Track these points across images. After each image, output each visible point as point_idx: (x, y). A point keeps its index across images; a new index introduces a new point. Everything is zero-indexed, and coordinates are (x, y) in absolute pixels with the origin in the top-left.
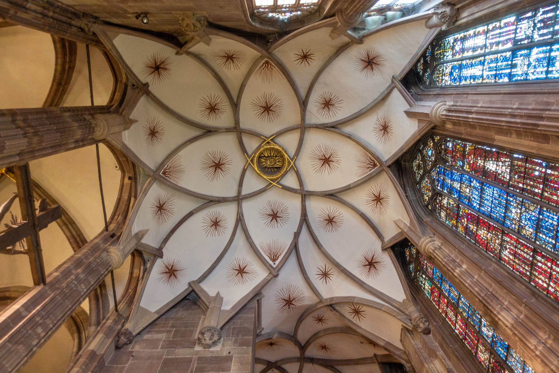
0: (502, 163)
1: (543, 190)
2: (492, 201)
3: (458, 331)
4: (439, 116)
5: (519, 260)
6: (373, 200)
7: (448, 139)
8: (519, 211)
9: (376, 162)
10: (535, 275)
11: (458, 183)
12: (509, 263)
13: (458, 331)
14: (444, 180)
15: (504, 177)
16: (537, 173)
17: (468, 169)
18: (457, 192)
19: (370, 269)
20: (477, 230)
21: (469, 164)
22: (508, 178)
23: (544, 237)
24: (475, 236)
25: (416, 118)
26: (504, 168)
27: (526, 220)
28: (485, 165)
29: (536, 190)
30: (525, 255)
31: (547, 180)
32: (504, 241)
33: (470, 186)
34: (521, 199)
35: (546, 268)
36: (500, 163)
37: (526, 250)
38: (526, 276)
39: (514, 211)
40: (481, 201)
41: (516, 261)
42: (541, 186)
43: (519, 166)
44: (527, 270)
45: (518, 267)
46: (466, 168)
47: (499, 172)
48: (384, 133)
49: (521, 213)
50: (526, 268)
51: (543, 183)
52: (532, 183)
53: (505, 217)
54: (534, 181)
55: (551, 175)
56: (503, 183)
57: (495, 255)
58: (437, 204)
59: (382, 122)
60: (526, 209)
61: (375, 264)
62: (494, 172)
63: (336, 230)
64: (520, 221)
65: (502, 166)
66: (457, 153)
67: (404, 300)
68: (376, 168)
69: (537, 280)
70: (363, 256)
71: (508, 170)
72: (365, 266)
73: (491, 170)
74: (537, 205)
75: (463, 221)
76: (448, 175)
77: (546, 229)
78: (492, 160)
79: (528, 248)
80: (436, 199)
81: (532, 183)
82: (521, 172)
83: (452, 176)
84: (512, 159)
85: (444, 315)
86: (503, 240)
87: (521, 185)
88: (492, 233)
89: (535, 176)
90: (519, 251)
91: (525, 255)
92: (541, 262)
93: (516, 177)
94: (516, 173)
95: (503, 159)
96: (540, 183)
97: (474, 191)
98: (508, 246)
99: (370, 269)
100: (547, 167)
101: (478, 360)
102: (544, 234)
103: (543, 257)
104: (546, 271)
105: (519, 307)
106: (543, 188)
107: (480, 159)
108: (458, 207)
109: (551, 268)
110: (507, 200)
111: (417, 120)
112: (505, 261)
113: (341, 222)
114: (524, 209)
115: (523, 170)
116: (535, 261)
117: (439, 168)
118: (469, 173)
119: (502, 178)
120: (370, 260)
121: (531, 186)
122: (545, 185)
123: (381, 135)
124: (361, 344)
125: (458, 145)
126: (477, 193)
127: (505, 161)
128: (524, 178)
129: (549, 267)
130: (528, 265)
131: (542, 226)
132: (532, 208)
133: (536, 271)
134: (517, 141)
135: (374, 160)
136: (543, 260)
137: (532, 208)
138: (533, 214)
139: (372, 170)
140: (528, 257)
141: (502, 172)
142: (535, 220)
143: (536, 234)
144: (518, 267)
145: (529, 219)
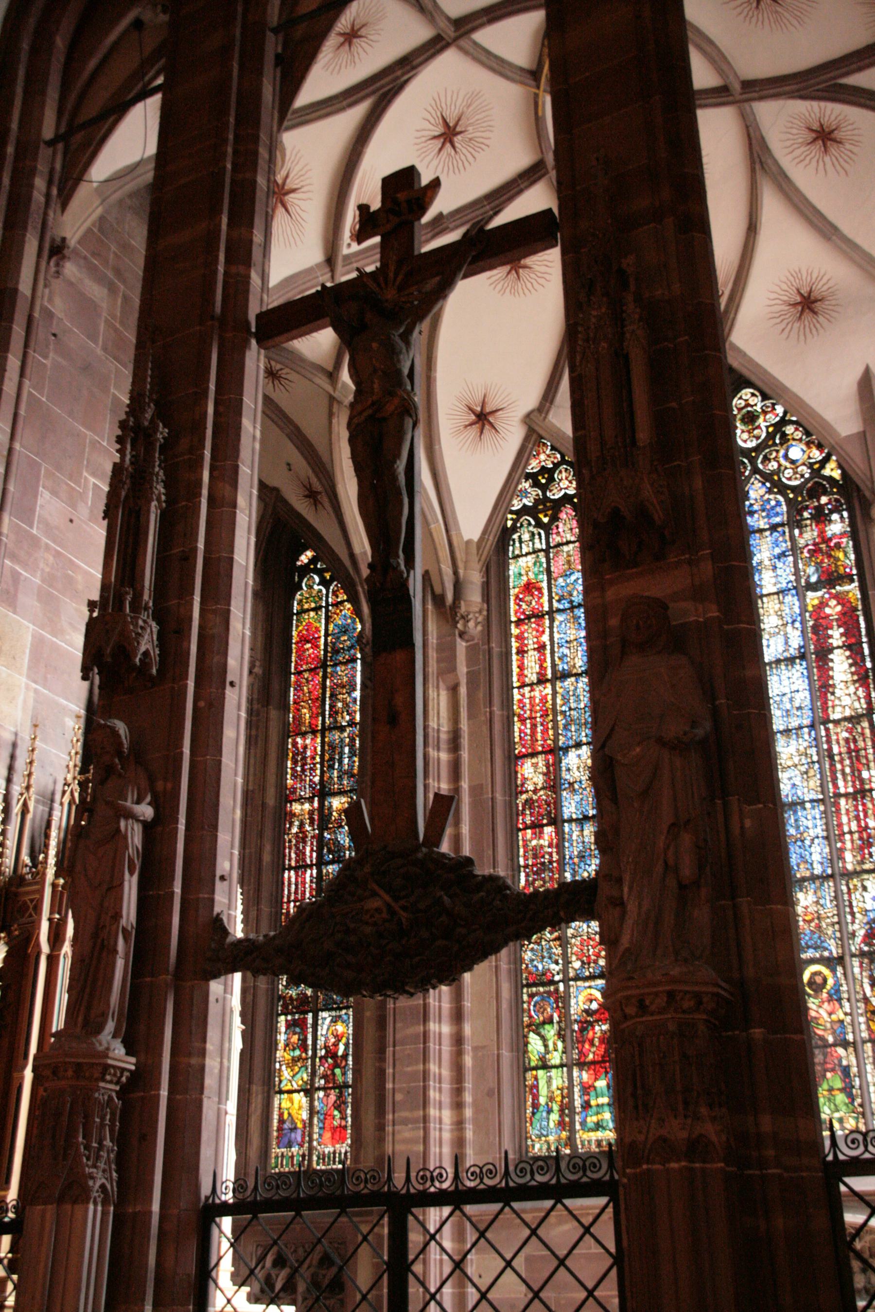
0: (855, 693)
1: (846, 795)
2: (784, 695)
3: (520, 697)
11: (775, 584)
13: (520, 697)
15: (833, 707)
17: (813, 606)
19: (471, 424)
21: (823, 604)
25: (865, 421)
27: (790, 779)
28: (836, 651)
29: (841, 783)
31: (863, 798)
33: (785, 625)
34: (815, 758)
36: (852, 689)
42: (851, 790)
43: (863, 734)
47: (838, 693)
51: (856, 792)
54: (853, 771)
56: (825, 708)
59: (820, 289)
60: (806, 773)
61: (487, 427)
63: (503, 291)
65: (849, 695)
66: (830, 556)
67: (469, 542)
70: (486, 389)
72: (470, 409)
74: (822, 792)
76: (776, 544)
77: (796, 820)
78: (851, 665)
82: (855, 741)
83: (779, 557)
85: (515, 644)
87: (836, 750)
89: (860, 772)
94: (850, 731)
96: (854, 786)
97: (781, 639)
99: (471, 424)
101: (516, 765)
106: (849, 794)
107: (842, 635)
110: (800, 728)
111: (861, 429)
113: (526, 291)
114: (803, 769)
115: (861, 744)
117: (778, 504)
118: (806, 611)
119: (830, 704)
120: (488, 410)
121: (843, 771)
122: (854, 796)
123: (786, 298)
124: (286, 467)
125: (846, 554)
128: (849, 751)
132: (812, 784)
138: (806, 790)
141: (839, 699)
142: (798, 797)
145: (794, 785)
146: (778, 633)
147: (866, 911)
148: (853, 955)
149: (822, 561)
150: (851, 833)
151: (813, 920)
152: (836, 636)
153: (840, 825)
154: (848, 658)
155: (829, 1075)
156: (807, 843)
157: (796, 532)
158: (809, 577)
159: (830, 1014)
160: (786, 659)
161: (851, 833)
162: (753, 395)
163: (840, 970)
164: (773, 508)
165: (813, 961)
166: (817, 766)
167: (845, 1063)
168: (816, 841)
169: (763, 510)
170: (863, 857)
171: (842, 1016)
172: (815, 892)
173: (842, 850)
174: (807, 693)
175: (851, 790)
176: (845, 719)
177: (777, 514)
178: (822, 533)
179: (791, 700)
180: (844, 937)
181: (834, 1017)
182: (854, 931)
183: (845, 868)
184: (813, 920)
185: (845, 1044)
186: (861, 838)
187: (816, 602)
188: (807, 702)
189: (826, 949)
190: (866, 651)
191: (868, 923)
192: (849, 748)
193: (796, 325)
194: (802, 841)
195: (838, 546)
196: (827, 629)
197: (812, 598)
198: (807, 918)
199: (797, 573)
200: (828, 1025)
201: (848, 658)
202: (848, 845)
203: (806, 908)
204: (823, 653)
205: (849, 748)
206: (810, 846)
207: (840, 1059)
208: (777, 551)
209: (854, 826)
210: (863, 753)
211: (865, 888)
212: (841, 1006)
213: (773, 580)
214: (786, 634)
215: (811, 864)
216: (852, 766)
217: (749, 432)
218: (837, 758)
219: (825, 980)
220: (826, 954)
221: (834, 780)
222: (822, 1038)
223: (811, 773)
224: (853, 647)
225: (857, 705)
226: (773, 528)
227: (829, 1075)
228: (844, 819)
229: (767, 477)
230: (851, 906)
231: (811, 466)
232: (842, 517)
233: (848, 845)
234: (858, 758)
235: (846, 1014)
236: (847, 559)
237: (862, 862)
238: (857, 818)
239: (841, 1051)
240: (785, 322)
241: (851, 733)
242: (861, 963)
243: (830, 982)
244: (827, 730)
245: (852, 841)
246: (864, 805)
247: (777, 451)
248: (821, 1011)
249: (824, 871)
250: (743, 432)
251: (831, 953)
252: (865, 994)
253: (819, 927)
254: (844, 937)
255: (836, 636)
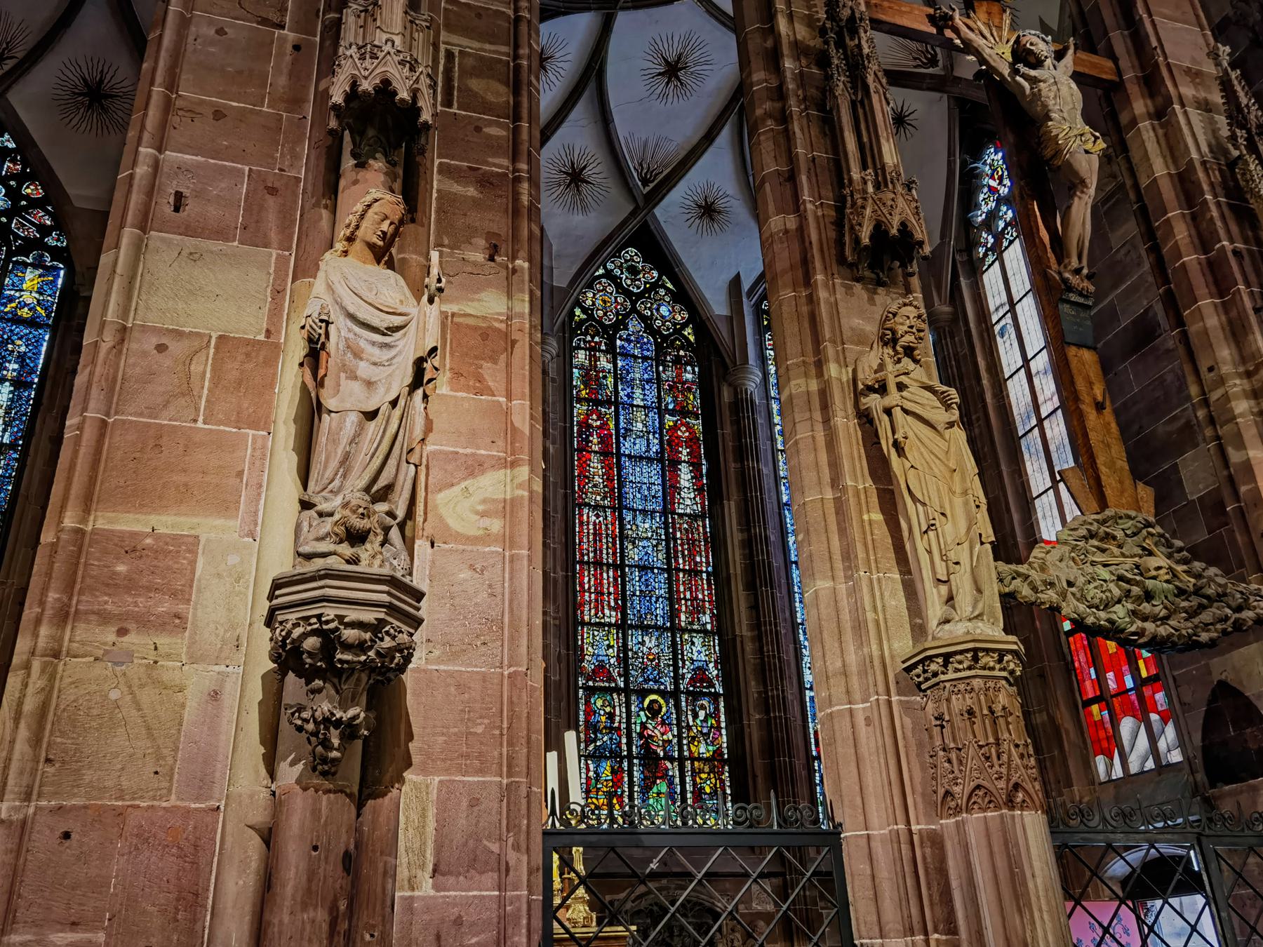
0: (694, 498)
1: (684, 571)
4: (744, 384)
5: (595, 540)
6: (573, 164)
7: (696, 369)
8: (650, 535)
9: (652, 185)
10: (589, 571)
12: (581, 523)
14: (636, 357)
15: (679, 503)
16: (698, 559)
18: (628, 396)
20: (596, 452)
21: (675, 428)
22: (680, 511)
23: (637, 579)
24: (584, 448)
26: (688, 502)
27: (644, 547)
29: (681, 561)
30: (605, 552)
31: (696, 576)
32: (605, 512)
33: (648, 433)
34: (663, 537)
35: (606, 586)
36: (692, 495)
37: (610, 551)
38: (582, 555)
39: (647, 526)
40: (635, 457)
41: (591, 537)
42: (687, 568)
44: (588, 555)
45: (585, 540)
46: (669, 420)
48: (700, 207)
49: (647, 538)
50: (591, 555)
52: (686, 552)
53: (635, 511)
55: (702, 579)
57: (580, 497)
58: (593, 337)
59: (720, 204)
62: (679, 482)
64: (641, 539)
68: (640, 183)
69: (586, 573)
71: (688, 511)
73: (679, 476)
75: (594, 417)
78: (692, 478)
79: (614, 553)
80: (597, 334)
81: (686, 552)
82: (693, 534)
84: (703, 517)
86: (604, 508)
87: (678, 535)
88: (604, 487)
89: (695, 556)
90: (604, 541)
91: (605, 552)
92: (608, 577)
93: (685, 526)
95: (698, 499)
96: (690, 565)
98: (601, 519)
100: (707, 572)
102: (640, 577)
103: (615, 579)
104: (601, 584)
105: (558, 569)
108: (608, 403)
109: (609, 594)
110: (654, 512)
112: (581, 515)
114: (654, 542)
116: (605, 568)
121: (683, 552)
126: (644, 449)
127: (697, 504)
128: (688, 539)
129: (608, 589)
130: (595, 557)
131: (646, 573)
133: (595, 570)
134: (736, 543)
135: (656, 182)
136: (611, 580)
137: (660, 556)
139: (635, 175)
140: (605, 556)
143: (635, 566)
144: (585, 540)
145: (647, 553)
146: (642, 437)
147: (693, 661)
148: (683, 692)
149: (677, 397)
150: (686, 600)
151: (654, 659)
152: (684, 453)
153: (678, 592)
154: (691, 471)
155: (658, 781)
156: (654, 599)
157: (661, 368)
158: (668, 404)
159: (663, 734)
160: (647, 458)
161: (686, 600)
162: (636, 254)
163: (672, 702)
164: (645, 343)
165: (652, 691)
166: (664, 543)
167: (671, 773)
168: (661, 600)
169: (638, 343)
170: (693, 621)
171: (671, 738)
172: (657, 639)
173: (679, 610)
174: (660, 488)
175: (687, 568)
176: (686, 515)
177: (648, 350)
178: (679, 375)
179: (649, 489)
180: (677, 678)
181: (665, 737)
182: (684, 674)
183: (679, 624)
184: (654, 659)
185: (672, 760)
186: (692, 605)
187: (671, 424)
188: (660, 494)
189: (662, 684)
190: (704, 471)
191: (693, 670)
192: (688, 536)
193: (697, 221)
194: (651, 597)
195: (689, 389)
196: (678, 445)
197: (669, 420)
198: (651, 657)
199: (659, 397)
200: (661, 743)
201: (691, 471)
202: (683, 608)
203: (650, 649)
204: (675, 463)
205: (688, 536)
206: (656, 602)
207: (667, 769)
208: (646, 376)
209: (688, 596)
210: (697, 543)
211: (693, 643)
212: (671, 730)
213: (641, 397)
214: (648, 440)
215: (656, 616)
216: (689, 550)
217: (631, 279)
218: (679, 542)
219: (660, 707)
220: (662, 687)
221: (676, 558)
222: (655, 752)
223: (660, 548)
224: (695, 466)
225: (695, 507)
226: (645, 358)
227: (658, 781)
228: (682, 589)
229: (643, 318)
230: (682, 654)
231: (675, 324)
232: (693, 370)
233: (683, 608)
234: (693, 543)
235: (674, 736)
236: (694, 401)
237: (692, 623)
238: (690, 589)
239: (669, 765)
240: (691, 215)
241: (690, 526)
242: (687, 700)
243: (664, 710)
244: (673, 519)
245: (686, 607)
246: (696, 581)
247: (652, 304)
248: (656, 731)
249: (664, 624)
250: (627, 278)
251: (666, 688)
252: (688, 723)
253: (658, 665)
254: (677, 678)
255: (684, 453)
